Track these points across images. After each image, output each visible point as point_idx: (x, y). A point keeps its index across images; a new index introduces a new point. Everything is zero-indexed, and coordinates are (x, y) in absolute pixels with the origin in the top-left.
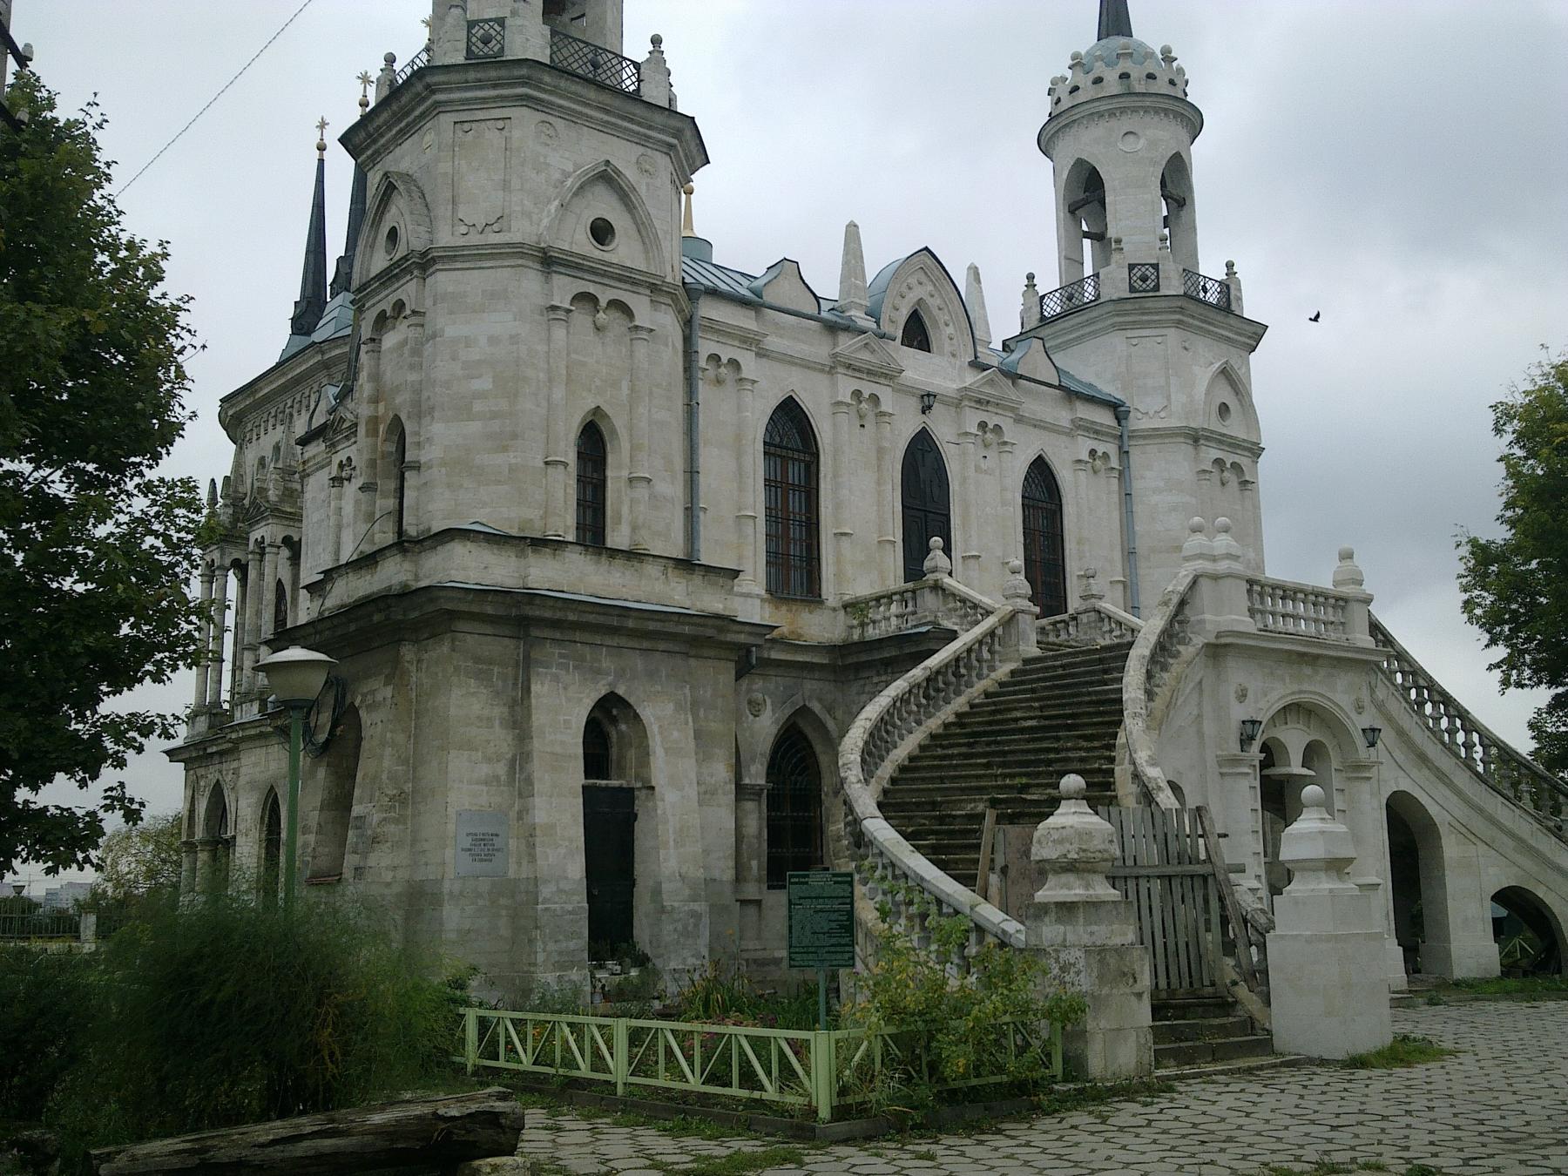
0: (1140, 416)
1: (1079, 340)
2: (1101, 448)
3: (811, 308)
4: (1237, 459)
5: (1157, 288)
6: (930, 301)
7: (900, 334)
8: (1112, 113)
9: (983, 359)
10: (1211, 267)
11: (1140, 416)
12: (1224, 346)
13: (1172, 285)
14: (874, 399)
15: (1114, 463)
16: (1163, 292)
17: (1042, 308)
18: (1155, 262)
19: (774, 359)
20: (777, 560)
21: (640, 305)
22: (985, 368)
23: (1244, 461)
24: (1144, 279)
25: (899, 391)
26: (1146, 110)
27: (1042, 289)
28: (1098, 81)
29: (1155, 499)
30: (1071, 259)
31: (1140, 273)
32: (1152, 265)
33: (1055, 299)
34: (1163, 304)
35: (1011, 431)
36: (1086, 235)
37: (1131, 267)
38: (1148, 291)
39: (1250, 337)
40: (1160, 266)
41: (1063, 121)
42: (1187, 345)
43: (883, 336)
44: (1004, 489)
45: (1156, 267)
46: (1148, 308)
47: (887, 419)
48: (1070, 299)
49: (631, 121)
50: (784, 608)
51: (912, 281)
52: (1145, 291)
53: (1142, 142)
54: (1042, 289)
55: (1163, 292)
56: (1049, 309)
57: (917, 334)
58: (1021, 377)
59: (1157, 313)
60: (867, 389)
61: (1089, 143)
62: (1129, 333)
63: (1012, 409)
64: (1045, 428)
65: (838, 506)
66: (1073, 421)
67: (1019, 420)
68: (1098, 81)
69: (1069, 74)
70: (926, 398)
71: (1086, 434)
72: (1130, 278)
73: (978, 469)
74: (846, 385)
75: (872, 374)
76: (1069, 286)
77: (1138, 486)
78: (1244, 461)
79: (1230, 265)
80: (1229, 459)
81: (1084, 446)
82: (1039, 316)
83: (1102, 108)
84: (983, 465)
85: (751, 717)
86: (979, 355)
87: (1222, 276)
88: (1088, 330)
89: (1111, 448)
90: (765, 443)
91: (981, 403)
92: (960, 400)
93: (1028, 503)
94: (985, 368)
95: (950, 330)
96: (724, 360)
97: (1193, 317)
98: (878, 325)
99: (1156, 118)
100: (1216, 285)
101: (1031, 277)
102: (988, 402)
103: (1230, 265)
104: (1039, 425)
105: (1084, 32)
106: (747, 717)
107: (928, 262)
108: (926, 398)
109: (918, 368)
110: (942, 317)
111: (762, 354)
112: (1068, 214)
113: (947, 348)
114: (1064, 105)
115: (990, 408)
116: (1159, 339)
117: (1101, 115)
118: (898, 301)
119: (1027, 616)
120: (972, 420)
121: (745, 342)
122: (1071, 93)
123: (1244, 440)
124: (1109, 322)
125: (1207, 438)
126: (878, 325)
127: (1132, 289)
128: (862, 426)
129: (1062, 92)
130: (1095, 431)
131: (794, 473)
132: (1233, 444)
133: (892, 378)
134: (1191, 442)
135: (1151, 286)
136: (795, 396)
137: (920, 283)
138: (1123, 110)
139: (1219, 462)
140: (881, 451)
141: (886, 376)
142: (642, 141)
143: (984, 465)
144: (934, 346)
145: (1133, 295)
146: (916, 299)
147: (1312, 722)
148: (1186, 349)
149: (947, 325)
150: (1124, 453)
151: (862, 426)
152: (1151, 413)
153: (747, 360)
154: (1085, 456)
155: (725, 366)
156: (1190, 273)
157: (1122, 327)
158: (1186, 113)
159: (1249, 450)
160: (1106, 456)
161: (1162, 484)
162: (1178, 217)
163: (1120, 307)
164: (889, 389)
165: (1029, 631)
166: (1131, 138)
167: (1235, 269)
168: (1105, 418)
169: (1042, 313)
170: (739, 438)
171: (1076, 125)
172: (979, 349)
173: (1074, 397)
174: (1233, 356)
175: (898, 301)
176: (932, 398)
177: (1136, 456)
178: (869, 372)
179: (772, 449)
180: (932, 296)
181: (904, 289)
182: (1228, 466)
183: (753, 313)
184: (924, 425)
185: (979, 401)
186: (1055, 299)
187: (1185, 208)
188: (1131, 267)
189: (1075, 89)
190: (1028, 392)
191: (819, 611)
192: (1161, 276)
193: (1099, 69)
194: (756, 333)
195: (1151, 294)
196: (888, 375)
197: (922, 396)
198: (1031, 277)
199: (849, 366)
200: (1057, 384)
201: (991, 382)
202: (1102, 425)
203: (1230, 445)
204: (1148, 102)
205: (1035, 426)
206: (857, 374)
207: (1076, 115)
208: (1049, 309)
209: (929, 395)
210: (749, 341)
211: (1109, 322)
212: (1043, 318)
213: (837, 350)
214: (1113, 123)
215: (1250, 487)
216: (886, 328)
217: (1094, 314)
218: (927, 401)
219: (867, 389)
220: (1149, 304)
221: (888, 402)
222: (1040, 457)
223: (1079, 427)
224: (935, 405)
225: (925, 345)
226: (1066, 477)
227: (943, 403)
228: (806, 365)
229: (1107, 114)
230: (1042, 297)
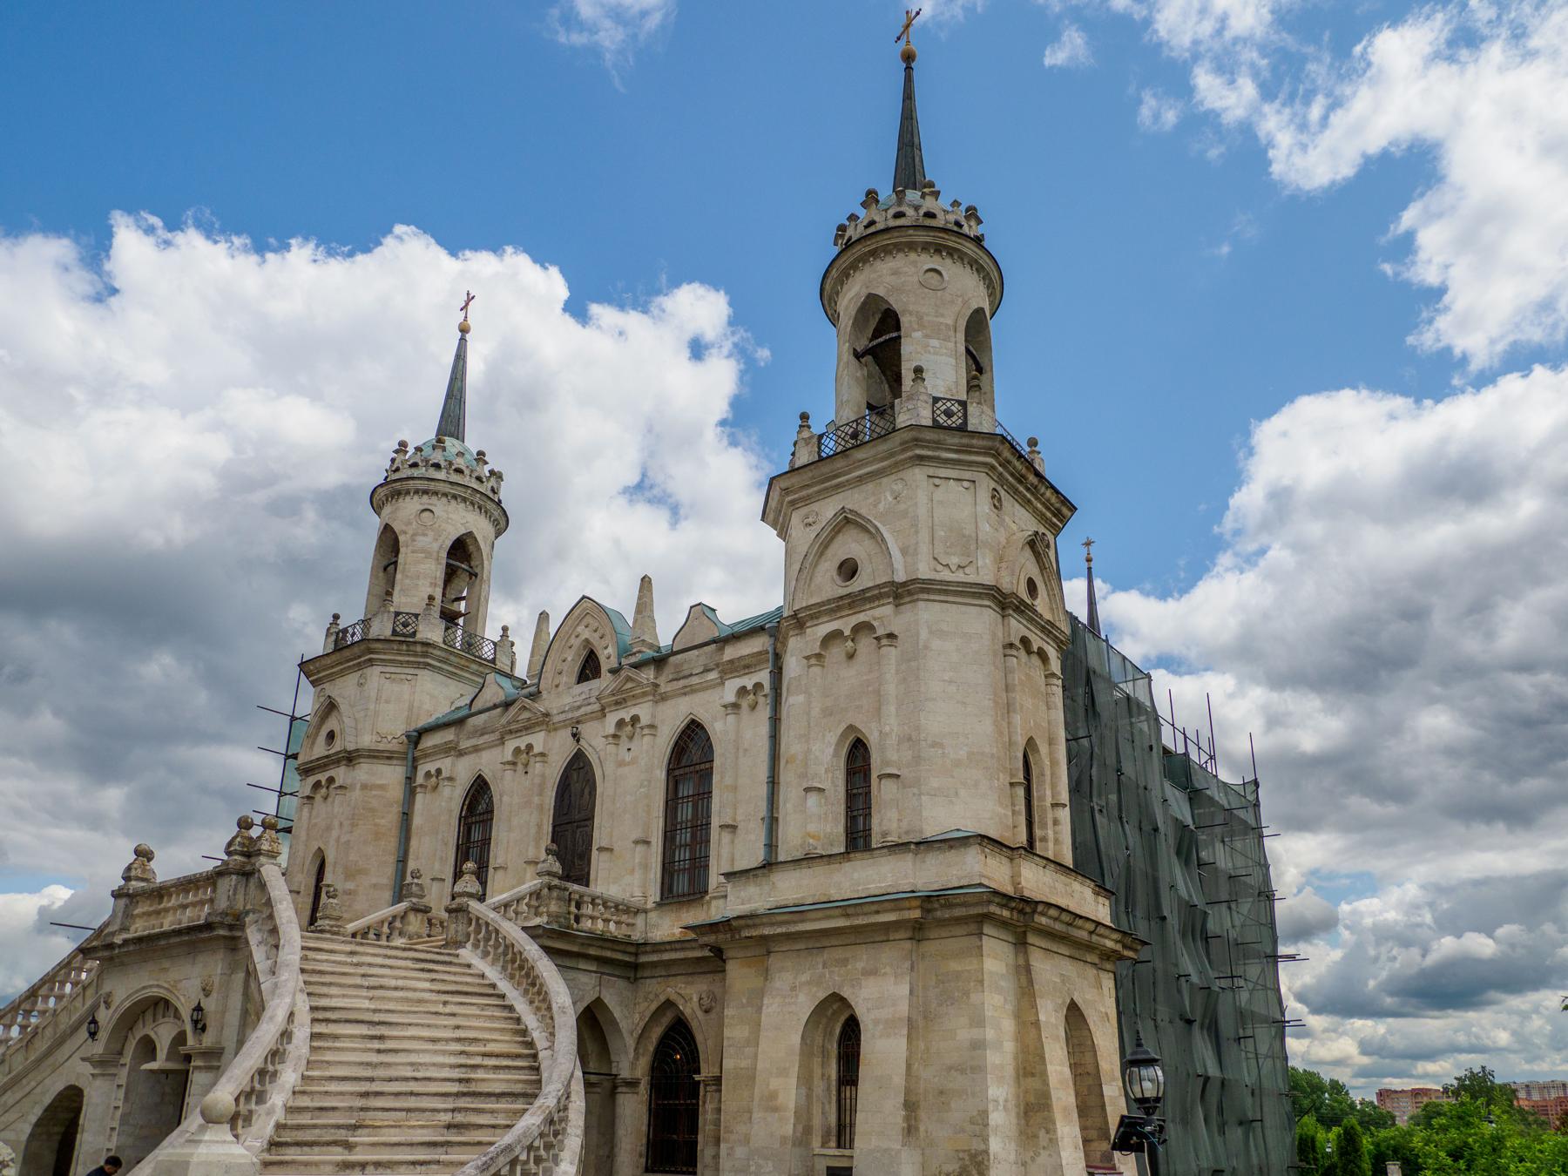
2: (749, 682)
4: (862, 617)
19: (470, 753)
21: (341, 774)
42: (810, 520)
49: (351, 660)
71: (736, 674)
75: (528, 728)
95: (606, 652)
102: (624, 699)
115: (629, 704)
125: (812, 617)
141: (537, 724)
142: (360, 667)
143: (628, 757)
153: (445, 764)
181: (573, 641)
199: (511, 732)
205: (685, 694)
206: (519, 734)
222: (693, 721)
226: (719, 729)
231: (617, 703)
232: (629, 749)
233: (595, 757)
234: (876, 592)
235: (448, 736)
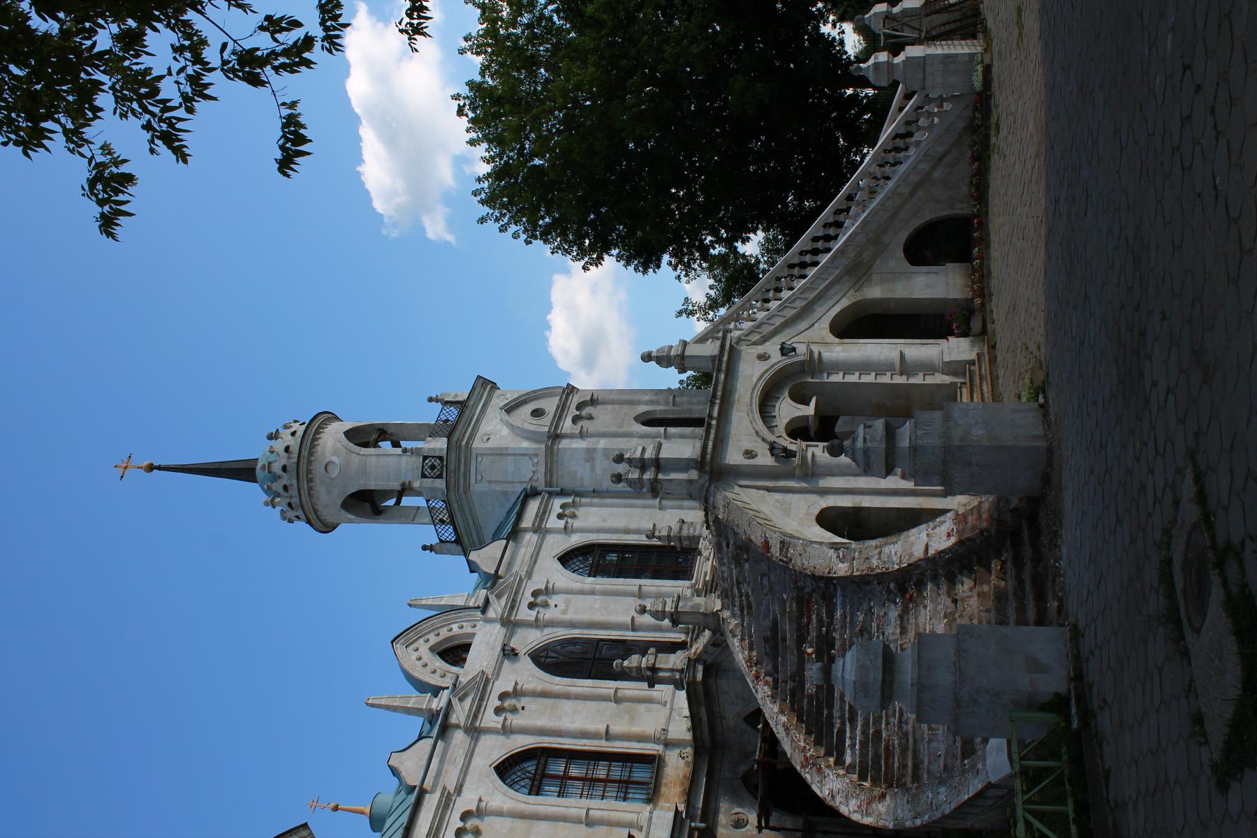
0: (535, 478)
1: (474, 518)
3: (428, 743)
4: (573, 406)
5: (441, 458)
6: (433, 639)
7: (454, 669)
8: (310, 480)
9: (481, 602)
10: (431, 414)
11: (535, 478)
12: (489, 410)
13: (439, 444)
14: (503, 696)
15: (569, 500)
16: (444, 454)
17: (448, 542)
18: (421, 458)
19: (464, 780)
20: (625, 788)
22: (487, 602)
23: (576, 400)
24: (433, 467)
25: (498, 675)
26: (311, 454)
27: (435, 541)
28: (285, 488)
29: (599, 471)
30: (411, 516)
31: (428, 470)
32: (424, 461)
33: (443, 532)
34: (453, 455)
35: (537, 582)
36: (398, 502)
37: (424, 476)
38: (443, 465)
39: (485, 389)
40: (425, 455)
41: (312, 517)
42: (485, 439)
43: (455, 685)
44: (582, 592)
45: (425, 458)
46: (455, 466)
47: (519, 687)
48: (442, 521)
50: (663, 789)
51: (416, 655)
52: (442, 467)
53: (335, 459)
54: (435, 541)
55: (444, 454)
56: (450, 537)
57: (455, 653)
58: (497, 571)
59: (459, 461)
60: (494, 702)
61: (328, 500)
62: (473, 481)
63: (521, 580)
64: (538, 554)
65: (585, 735)
66: (535, 532)
67: (529, 575)
68: (285, 488)
69: (278, 509)
70: (506, 652)
72: (432, 477)
73: (564, 612)
74: (489, 719)
76: (434, 522)
77: (588, 484)
78: (576, 400)
79: (431, 400)
80: (573, 411)
81: (553, 522)
82: (454, 544)
83: (306, 487)
84: (562, 608)
85: (748, 826)
86: (476, 605)
87: (439, 406)
88: (467, 512)
89: (557, 503)
90: (530, 794)
91: (513, 606)
92: (510, 624)
93: (596, 571)
94: (487, 602)
95: (455, 627)
96: (460, 824)
97: (465, 432)
98: (447, 688)
99: (319, 448)
100: (444, 412)
101: (425, 548)
103: (431, 400)
104: (535, 559)
105: (251, 492)
106: (748, 830)
107: (402, 641)
108: (506, 652)
109: (480, 658)
110: (444, 633)
111: (459, 789)
112: (382, 516)
113: (470, 630)
114: (300, 513)
116: (479, 459)
117: (310, 489)
118: (429, 669)
119: (681, 604)
120: (524, 613)
121: (449, 805)
122: (292, 509)
123: (560, 400)
124: (463, 496)
125: (557, 427)
126: (447, 688)
127: (440, 476)
128: (523, 708)
129: (291, 514)
130: (543, 514)
131: (557, 767)
132: (562, 409)
133: (487, 680)
134: (558, 440)
135: (439, 462)
136: (494, 765)
137: (417, 650)
138: (309, 472)
139: (575, 420)
140: (544, 694)
141: (485, 686)
143: (562, 607)
144: (467, 641)
145: (445, 476)
146: (430, 654)
147: (769, 404)
148: (489, 439)
149: (451, 629)
150: (563, 493)
151: (523, 708)
152: (534, 469)
153: (466, 801)
154: (561, 524)
155: (465, 823)
156: (432, 431)
157: (467, 487)
158: (317, 425)
159: (568, 395)
160: (563, 506)
161: (588, 465)
162: (391, 434)
163: (451, 487)
164: (497, 683)
165: (693, 603)
166: (329, 467)
167: (434, 396)
168: (533, 506)
169: (452, 542)
170: (522, 816)
171: (317, 507)
172: (471, 604)
173: (516, 528)
174: (498, 402)
175: (429, 669)
176: (507, 648)
177: (567, 483)
178: (481, 699)
179: (536, 790)
180: (428, 640)
182: (578, 413)
183: (427, 796)
184: (526, 655)
185: (512, 608)
186: (443, 532)
187: (385, 429)
188: (424, 476)
189: (290, 505)
190: (510, 565)
191: (667, 759)
192: (433, 455)
193: (278, 486)
194: (442, 794)
195: (445, 463)
196: (483, 683)
197: (504, 655)
198: (425, 548)
199: (475, 717)
200: (505, 541)
201: (499, 596)
202: (539, 508)
203: (563, 410)
204: (305, 453)
205: (535, 562)
207: (308, 507)
208: (450, 537)
209: (503, 650)
210: (447, 802)
211: (463, 496)
212: (455, 542)
213: (462, 724)
214: (317, 480)
215: (595, 397)
216: (448, 682)
217: (455, 506)
218: (509, 653)
219: (494, 702)
220: (452, 466)
221: (504, 684)
223: (539, 526)
224: (512, 645)
225: (466, 647)
226: (576, 540)
227: (510, 639)
228: (470, 755)
229: (311, 484)
230: (441, 541)
231: (512, 608)
232: (556, 606)
233: (545, 638)
234: (564, 396)
235: (431, 803)
